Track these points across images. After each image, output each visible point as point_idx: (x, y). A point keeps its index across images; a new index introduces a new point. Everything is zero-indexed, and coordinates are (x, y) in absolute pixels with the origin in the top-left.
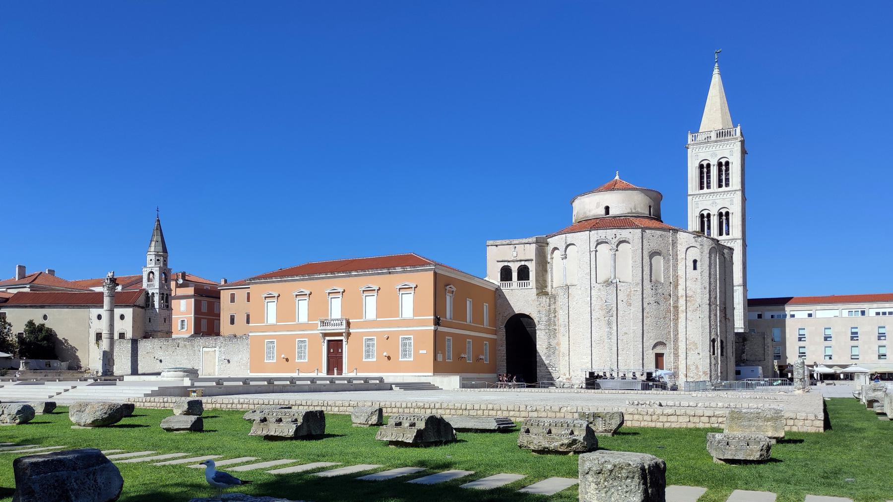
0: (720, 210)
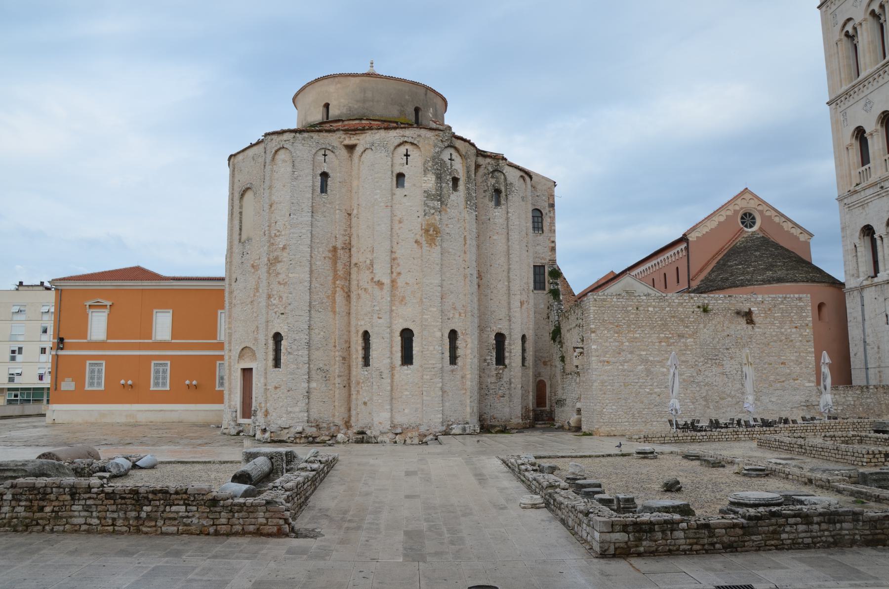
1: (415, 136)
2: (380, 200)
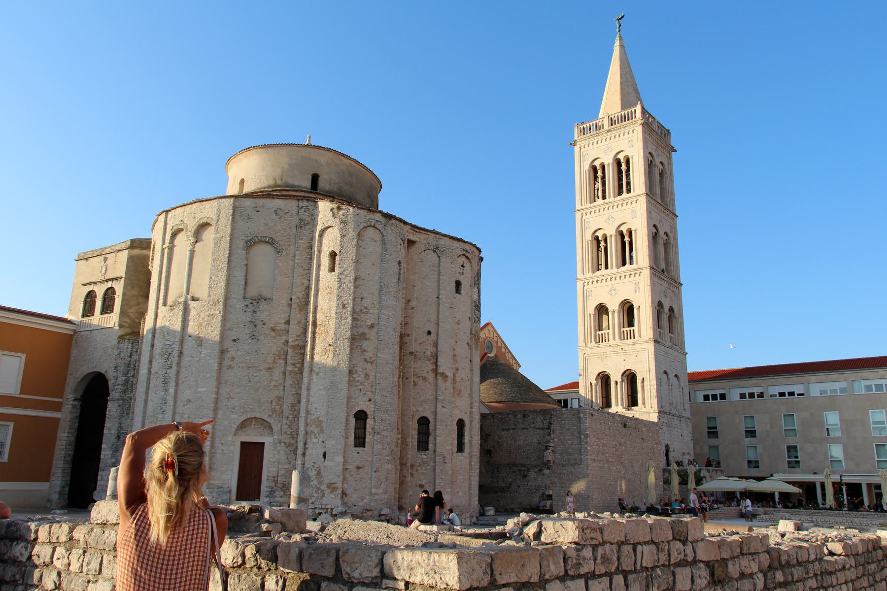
0: (619, 226)
1: (470, 252)
2: (445, 300)
